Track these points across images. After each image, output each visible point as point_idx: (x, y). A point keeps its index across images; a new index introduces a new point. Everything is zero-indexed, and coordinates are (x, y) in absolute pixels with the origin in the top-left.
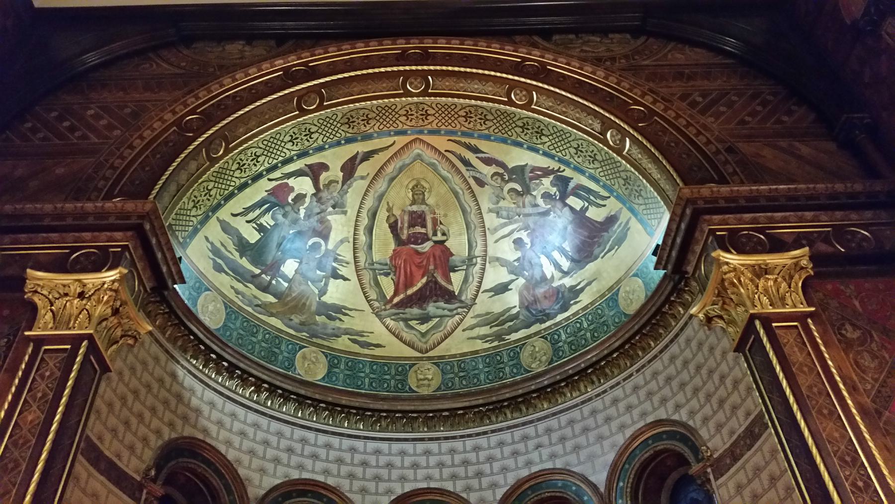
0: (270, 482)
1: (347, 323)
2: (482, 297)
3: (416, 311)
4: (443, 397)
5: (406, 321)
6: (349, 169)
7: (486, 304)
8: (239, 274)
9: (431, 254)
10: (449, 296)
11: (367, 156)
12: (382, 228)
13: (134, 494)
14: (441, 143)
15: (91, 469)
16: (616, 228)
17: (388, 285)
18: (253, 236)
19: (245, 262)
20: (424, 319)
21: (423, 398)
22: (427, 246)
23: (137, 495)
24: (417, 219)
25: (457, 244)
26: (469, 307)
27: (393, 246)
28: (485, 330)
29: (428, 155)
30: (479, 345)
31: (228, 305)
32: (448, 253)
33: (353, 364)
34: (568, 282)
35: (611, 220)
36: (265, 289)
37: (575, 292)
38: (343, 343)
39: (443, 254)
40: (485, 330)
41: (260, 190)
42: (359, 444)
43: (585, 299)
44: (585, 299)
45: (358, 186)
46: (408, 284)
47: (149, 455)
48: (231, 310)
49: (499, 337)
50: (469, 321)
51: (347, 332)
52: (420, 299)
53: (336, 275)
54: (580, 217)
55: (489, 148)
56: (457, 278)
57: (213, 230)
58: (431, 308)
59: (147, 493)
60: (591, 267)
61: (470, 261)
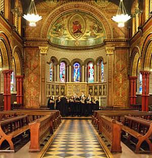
1: (67, 36)
6: (67, 17)
10: (81, 32)
18: (55, 28)
19: (55, 32)
21: (77, 47)
22: (78, 25)
24: (77, 21)
25: (82, 25)
26: (83, 34)
27: (73, 25)
32: (81, 26)
35: (101, 29)
37: (97, 36)
38: (67, 39)
39: (80, 26)
41: (55, 23)
43: (98, 37)
44: (98, 37)
45: (68, 18)
48: (54, 38)
52: (77, 32)
56: (82, 30)
58: (78, 33)
60: (98, 34)
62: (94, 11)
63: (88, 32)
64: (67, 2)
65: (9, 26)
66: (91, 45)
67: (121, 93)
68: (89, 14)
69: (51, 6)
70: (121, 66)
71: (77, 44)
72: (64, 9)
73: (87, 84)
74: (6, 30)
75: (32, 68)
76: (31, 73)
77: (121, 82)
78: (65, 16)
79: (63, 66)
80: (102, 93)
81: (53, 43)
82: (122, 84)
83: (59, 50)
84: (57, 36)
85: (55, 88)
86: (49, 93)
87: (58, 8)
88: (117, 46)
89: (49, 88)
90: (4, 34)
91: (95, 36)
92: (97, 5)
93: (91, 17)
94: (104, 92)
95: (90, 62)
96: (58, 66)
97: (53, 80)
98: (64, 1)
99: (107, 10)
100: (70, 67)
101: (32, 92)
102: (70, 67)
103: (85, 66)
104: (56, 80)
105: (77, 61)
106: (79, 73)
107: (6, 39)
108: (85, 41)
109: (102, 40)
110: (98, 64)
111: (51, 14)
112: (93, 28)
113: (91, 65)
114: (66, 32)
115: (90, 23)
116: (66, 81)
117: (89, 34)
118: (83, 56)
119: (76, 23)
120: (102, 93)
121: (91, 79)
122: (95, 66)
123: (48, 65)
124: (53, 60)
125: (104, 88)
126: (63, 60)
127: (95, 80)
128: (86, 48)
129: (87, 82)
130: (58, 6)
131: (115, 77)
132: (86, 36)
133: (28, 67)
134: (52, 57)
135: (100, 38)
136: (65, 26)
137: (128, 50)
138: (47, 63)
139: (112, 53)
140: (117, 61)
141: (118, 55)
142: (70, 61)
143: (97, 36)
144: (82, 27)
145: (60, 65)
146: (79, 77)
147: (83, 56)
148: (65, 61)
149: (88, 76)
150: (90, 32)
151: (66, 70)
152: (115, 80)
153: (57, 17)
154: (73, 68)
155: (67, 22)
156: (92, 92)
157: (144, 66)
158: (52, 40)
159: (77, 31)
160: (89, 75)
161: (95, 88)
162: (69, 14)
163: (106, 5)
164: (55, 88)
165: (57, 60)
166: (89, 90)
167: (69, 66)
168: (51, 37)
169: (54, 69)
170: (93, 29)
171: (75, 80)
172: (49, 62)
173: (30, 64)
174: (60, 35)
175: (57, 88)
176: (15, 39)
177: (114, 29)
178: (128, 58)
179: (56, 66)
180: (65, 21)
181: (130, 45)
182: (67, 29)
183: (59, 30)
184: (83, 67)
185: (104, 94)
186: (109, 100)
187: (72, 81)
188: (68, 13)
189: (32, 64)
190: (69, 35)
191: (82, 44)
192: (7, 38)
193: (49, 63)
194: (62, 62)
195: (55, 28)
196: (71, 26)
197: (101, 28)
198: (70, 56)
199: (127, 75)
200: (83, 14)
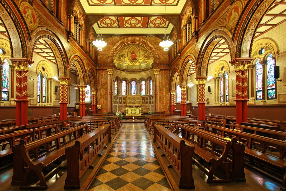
0: (122, 78)
1: (127, 62)
2: (139, 60)
3: (133, 61)
4: (135, 70)
5: (132, 62)
6: (127, 48)
7: (139, 61)
8: (118, 60)
9: (135, 55)
10: (136, 59)
11: (129, 47)
12: (130, 53)
14: (136, 46)
16: (150, 58)
17: (130, 58)
19: (118, 59)
20: (134, 62)
21: (133, 70)
22: (134, 54)
24: (133, 52)
25: (137, 54)
28: (139, 63)
29: (134, 47)
30: (139, 65)
31: (117, 63)
32: (136, 55)
33: (128, 66)
34: (147, 61)
35: (150, 57)
36: (120, 61)
38: (127, 64)
39: (136, 56)
40: (139, 63)
41: (119, 53)
42: (128, 74)
43: (148, 63)
45: (128, 49)
46: (132, 58)
47: (115, 79)
49: (140, 64)
50: (138, 62)
51: (127, 63)
52: (133, 60)
53: (126, 58)
54: (148, 55)
55: (140, 47)
56: (137, 58)
57: (116, 58)
58: (134, 60)
61: (138, 56)
62: (145, 44)
63: (141, 59)
64: (126, 37)
65: (83, 51)
66: (143, 68)
67: (164, 102)
68: (142, 46)
69: (116, 40)
70: (164, 83)
71: (134, 68)
72: (125, 42)
73: (141, 96)
74: (81, 54)
75: (103, 85)
76: (102, 88)
77: (164, 94)
78: (126, 48)
79: (124, 83)
80: (151, 102)
81: (118, 67)
82: (165, 95)
83: (122, 72)
84: (120, 62)
85: (119, 99)
86: (115, 102)
87: (121, 41)
88: (161, 68)
89: (115, 99)
90: (79, 57)
91: (146, 62)
92: (147, 39)
93: (143, 48)
94: (152, 102)
95: (142, 80)
96: (121, 83)
97: (118, 94)
98: (125, 37)
99: (154, 43)
100: (129, 84)
101: (103, 102)
102: (129, 84)
103: (139, 83)
104: (120, 94)
105: (134, 80)
106: (135, 89)
107: (80, 60)
108: (139, 66)
109: (151, 64)
110: (148, 82)
111: (115, 46)
112: (145, 56)
113: (143, 83)
114: (126, 59)
115: (142, 53)
116: (127, 94)
117: (142, 61)
118: (138, 76)
119: (133, 53)
120: (151, 102)
121: (143, 93)
122: (146, 83)
123: (114, 82)
124: (117, 79)
125: (152, 98)
126: (124, 79)
127: (146, 93)
128: (140, 71)
129: (141, 94)
130: (120, 40)
131: (160, 90)
132: (140, 62)
133: (99, 84)
134: (117, 77)
135: (149, 64)
136: (125, 55)
137: (169, 71)
138: (113, 81)
139: (158, 73)
140: (161, 80)
141: (162, 75)
142: (129, 80)
143: (147, 62)
144: (137, 56)
145: (122, 83)
146: (135, 91)
147: (138, 76)
148: (125, 80)
149: (142, 90)
150: (143, 59)
151: (126, 86)
152: (160, 92)
153: (120, 48)
154: (131, 85)
155: (127, 52)
157: (182, 81)
158: (116, 65)
159: (134, 59)
160: (142, 90)
161: (147, 99)
162: (128, 46)
163: (153, 39)
164: (119, 99)
165: (120, 79)
166: (142, 100)
167: (128, 83)
168: (116, 62)
169: (118, 85)
170: (145, 57)
173: (101, 82)
174: (122, 61)
175: (121, 98)
176: (89, 62)
177: (159, 56)
178: (169, 77)
179: (120, 83)
180: (125, 52)
181: (170, 67)
182: (127, 57)
183: (122, 58)
184: (138, 84)
185: (152, 103)
186: (157, 108)
187: (131, 94)
188: (127, 45)
189: (102, 82)
190: (128, 62)
191: (137, 68)
192: (82, 61)
193: (115, 81)
194: (124, 80)
195: (118, 56)
196: (130, 55)
197: (150, 56)
198: (130, 76)
199: (168, 89)
200: (138, 45)
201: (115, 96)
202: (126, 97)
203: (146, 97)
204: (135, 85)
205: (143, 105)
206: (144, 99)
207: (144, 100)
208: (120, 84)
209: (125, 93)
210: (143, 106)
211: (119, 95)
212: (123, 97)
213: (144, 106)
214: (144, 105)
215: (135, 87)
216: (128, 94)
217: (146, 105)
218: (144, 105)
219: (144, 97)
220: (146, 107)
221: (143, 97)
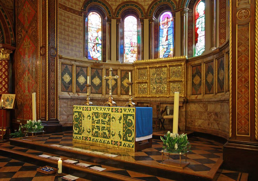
13: (80, 14)
15: (65, 11)
23: (81, 14)
59: (84, 14)
97: (104, 59)
106: (171, 37)
129: (190, 54)
146: (172, 47)
149: (193, 38)
156: (200, 84)
161: (210, 70)
166: (193, 76)
171: (161, 57)
172: (78, 8)
201: (86, 65)
202: (131, 68)
203: (206, 63)
204: (170, 23)
205: (193, 97)
206: (199, 73)
207: (201, 78)
208: (110, 25)
209: (135, 55)
210: (193, 102)
211: (108, 61)
212: (121, 71)
213: (199, 102)
214: (199, 97)
215: (171, 31)
216: (143, 59)
217: (208, 97)
218: (199, 97)
219: (200, 65)
220: (206, 107)
221: (197, 62)
